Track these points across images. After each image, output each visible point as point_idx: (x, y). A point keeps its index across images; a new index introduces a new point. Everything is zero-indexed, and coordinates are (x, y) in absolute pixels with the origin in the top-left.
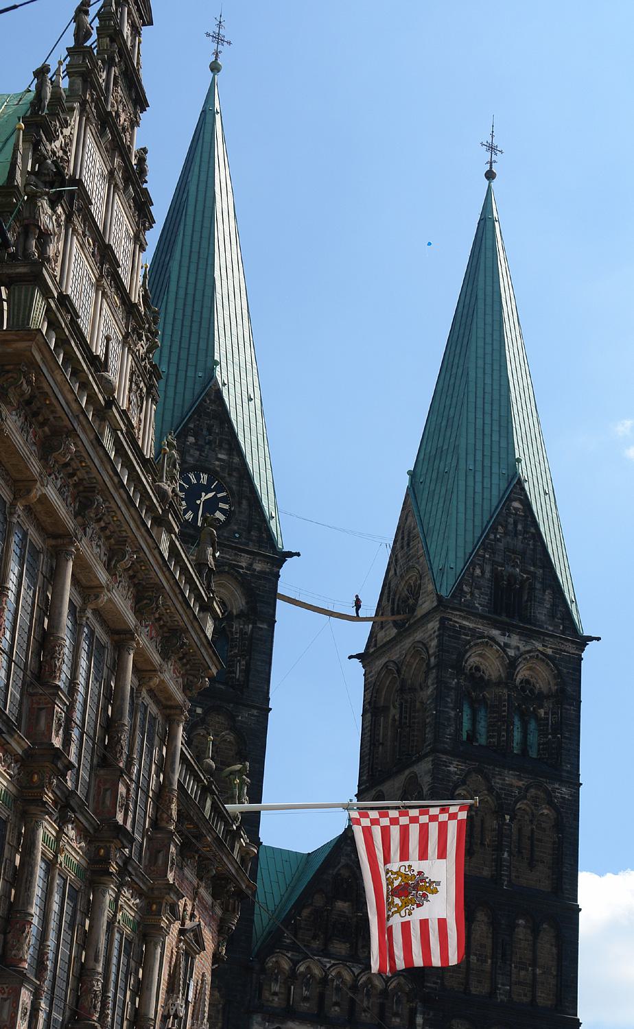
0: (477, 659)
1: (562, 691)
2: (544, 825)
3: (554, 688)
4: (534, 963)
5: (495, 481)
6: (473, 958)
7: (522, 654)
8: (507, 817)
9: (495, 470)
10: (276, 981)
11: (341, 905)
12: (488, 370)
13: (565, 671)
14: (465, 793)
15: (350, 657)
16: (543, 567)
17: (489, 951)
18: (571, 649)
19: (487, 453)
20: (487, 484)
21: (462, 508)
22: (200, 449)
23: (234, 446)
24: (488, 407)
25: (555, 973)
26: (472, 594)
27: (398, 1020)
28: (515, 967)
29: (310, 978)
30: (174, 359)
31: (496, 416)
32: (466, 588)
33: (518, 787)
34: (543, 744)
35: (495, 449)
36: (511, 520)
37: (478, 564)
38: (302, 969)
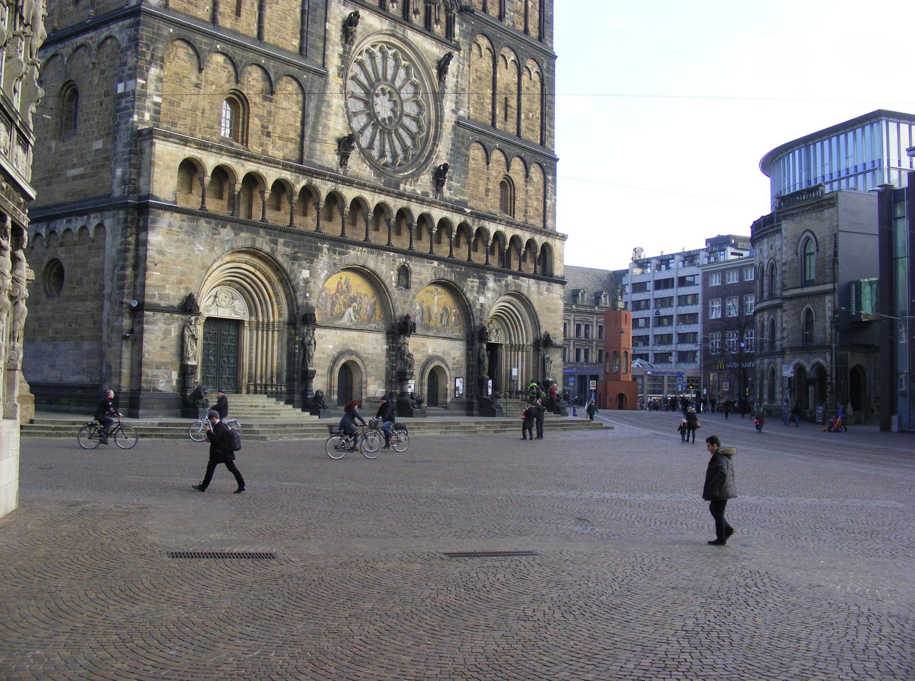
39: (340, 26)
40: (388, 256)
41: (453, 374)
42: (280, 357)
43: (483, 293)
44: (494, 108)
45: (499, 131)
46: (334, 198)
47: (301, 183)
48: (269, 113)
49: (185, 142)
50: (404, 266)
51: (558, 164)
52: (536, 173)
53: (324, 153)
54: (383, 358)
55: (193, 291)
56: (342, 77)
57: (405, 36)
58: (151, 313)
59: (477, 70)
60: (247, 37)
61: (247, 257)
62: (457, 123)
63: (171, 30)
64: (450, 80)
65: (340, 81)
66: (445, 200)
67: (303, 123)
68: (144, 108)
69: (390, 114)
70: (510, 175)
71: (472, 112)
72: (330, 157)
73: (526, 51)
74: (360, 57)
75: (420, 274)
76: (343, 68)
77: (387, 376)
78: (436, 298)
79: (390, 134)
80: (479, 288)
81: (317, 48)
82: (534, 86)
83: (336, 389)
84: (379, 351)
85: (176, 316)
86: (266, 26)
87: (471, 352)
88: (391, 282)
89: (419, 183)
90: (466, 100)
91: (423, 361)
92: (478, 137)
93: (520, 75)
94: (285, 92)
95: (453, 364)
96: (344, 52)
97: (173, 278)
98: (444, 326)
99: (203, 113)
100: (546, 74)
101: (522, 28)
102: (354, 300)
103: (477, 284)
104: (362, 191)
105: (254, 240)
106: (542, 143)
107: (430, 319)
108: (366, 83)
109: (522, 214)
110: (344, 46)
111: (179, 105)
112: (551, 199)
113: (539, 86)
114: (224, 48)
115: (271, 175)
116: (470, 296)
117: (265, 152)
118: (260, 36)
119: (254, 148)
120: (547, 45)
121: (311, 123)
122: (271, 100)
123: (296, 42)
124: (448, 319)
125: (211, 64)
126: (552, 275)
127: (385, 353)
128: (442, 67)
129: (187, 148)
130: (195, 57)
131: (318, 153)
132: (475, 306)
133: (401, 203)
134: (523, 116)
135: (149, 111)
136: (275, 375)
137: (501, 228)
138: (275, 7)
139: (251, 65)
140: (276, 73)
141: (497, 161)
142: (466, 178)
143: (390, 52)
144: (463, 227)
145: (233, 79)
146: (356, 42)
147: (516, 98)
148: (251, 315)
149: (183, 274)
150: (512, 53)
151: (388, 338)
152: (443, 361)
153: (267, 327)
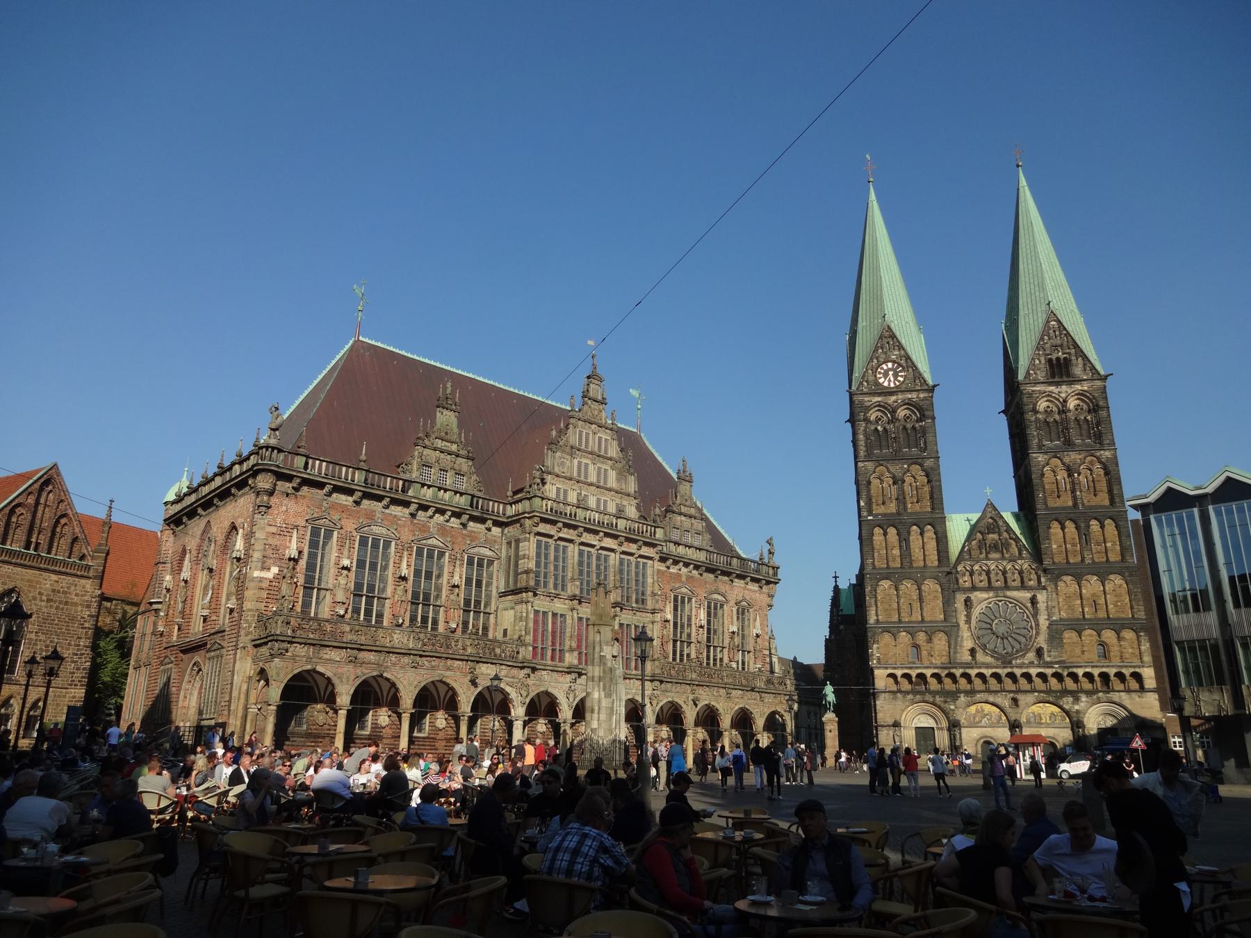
4: (1105, 542)
5: (1039, 315)
6: (1068, 546)
8: (1076, 475)
9: (1039, 309)
11: (991, 536)
12: (1030, 262)
18: (1098, 383)
19: (1034, 303)
20: (1035, 318)
22: (886, 353)
23: (901, 347)
24: (1032, 281)
26: (1035, 373)
30: (868, 318)
31: (1036, 283)
32: (1031, 372)
33: (1080, 459)
35: (1038, 300)
36: (1051, 331)
44: (1083, 609)
49: (886, 668)
62: (1050, 624)
64: (1042, 606)
65: (967, 626)
66: (1047, 663)
72: (966, 658)
86: (925, 614)
90: (1057, 611)
92: (1069, 627)
93: (1103, 586)
97: (888, 715)
101: (1105, 559)
102: (987, 715)
107: (1041, 719)
116: (1067, 707)
117: (932, 663)
123: (942, 616)
128: (1033, 601)
134: (1111, 606)
141: (1091, 635)
143: (1000, 604)
152: (1053, 738)
153: (942, 729)
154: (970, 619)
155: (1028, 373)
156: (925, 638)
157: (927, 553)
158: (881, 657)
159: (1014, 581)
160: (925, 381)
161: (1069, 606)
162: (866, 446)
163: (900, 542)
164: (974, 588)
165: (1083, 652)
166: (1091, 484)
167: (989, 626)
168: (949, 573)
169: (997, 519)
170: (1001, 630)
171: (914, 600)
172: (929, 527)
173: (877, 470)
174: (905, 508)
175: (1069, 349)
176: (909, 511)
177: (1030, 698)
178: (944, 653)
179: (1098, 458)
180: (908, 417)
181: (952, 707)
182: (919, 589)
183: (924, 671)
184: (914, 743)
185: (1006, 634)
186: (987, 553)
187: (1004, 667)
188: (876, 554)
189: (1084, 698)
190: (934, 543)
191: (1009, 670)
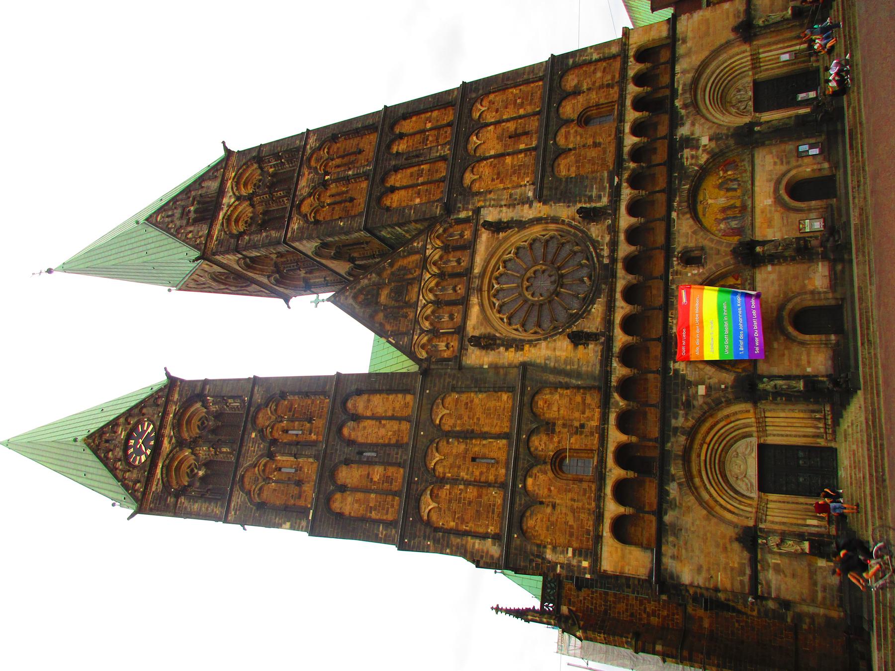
0: (240, 224)
1: (254, 158)
2: (335, 150)
3: (256, 166)
4: (423, 131)
6: (421, 180)
7: (234, 194)
8: (327, 177)
10: (436, 346)
13: (244, 161)
14: (313, 215)
15: (289, 307)
16: (190, 191)
17: (416, 168)
18: (233, 159)
21: (162, 254)
25: (430, 114)
26: (200, 237)
27: (466, 233)
28: (426, 145)
29: (434, 316)
32: (198, 242)
33: (309, 174)
34: (288, 164)
37: (186, 236)
38: (427, 324)
39: (484, 352)
40: (673, 281)
41: (794, 163)
42: (793, 410)
43: (698, 140)
44: (521, 152)
45: (539, 142)
46: (628, 356)
47: (619, 402)
48: (564, 425)
49: (598, 538)
50: (681, 257)
51: (557, 53)
52: (571, 81)
53: (588, 362)
54: (783, 268)
55: (734, 535)
56: (523, 346)
57: (479, 277)
58: (760, 586)
59: (493, 180)
60: (508, 454)
61: (694, 456)
63: (516, 536)
64: (506, 214)
65: (527, 347)
66: (610, 201)
67: (567, 387)
68: (579, 566)
69: (546, 274)
70: (575, 116)
71: (528, 179)
72: (591, 354)
73: (466, 123)
74: (505, 320)
75: (687, 235)
76: (517, 346)
77: (804, 263)
78: (710, 201)
79: (562, 276)
80: (692, 148)
81: (506, 375)
82: (494, 103)
83: (823, 337)
84: (773, 276)
85: (759, 556)
86: (496, 430)
87: (767, 142)
88: (699, 275)
89: (599, 239)
90: (518, 191)
91: (782, 211)
92: (549, 169)
94: (545, 409)
95: (782, 163)
96: (503, 345)
98: (739, 185)
99: (573, 500)
100: (481, 92)
101: (449, 130)
103: (688, 150)
104: (615, 323)
105: (677, 456)
106: (541, 79)
107: (733, 207)
108: (526, 308)
109: (612, 91)
110: (499, 346)
111: (571, 527)
112: (591, 54)
113: (492, 97)
114: (521, 480)
115: (616, 437)
116: (703, 158)
118: (506, 436)
119: (595, 442)
120: (456, 96)
121: (567, 380)
122: (554, 424)
123: (505, 397)
124: (732, 181)
125: (535, 491)
126: (667, 38)
127: (777, 268)
128: (497, 227)
129: (605, 534)
130: (532, 509)
131: (589, 369)
132: (712, 149)
133: (620, 271)
134: (522, 112)
135: (580, 562)
136: (813, 415)
137: (627, 129)
138: (482, 422)
139: (529, 448)
140: (532, 422)
141: (566, 138)
142: (587, 177)
143: (496, 286)
144: (635, 182)
145: (543, 467)
146: (492, 331)
147: (509, 125)
148: (750, 436)
149: (718, 546)
150: (471, 139)
151: (759, 266)
152: (778, 182)
154: (514, 340)
155: (196, 247)
156: (545, 438)
157: (390, 413)
158: (575, 545)
159: (459, 262)
160: (160, 390)
161: (514, 173)
162: (210, 500)
163: (360, 462)
164: (460, 330)
165: (596, 145)
166: (346, 160)
167: (536, 308)
168: (425, 372)
169: (358, 287)
170: (545, 284)
171: (467, 450)
172: (350, 404)
173: (247, 486)
174: (314, 443)
175: (189, 197)
176: (321, 438)
177: (684, 227)
178: (579, 399)
179: (314, 151)
180: (203, 423)
181: (702, 390)
182: (448, 435)
183: (611, 448)
184: (802, 499)
185: (553, 278)
186: (408, 305)
187: (614, 275)
188: (374, 515)
189: (684, 131)
190: (377, 399)
191: (620, 265)
